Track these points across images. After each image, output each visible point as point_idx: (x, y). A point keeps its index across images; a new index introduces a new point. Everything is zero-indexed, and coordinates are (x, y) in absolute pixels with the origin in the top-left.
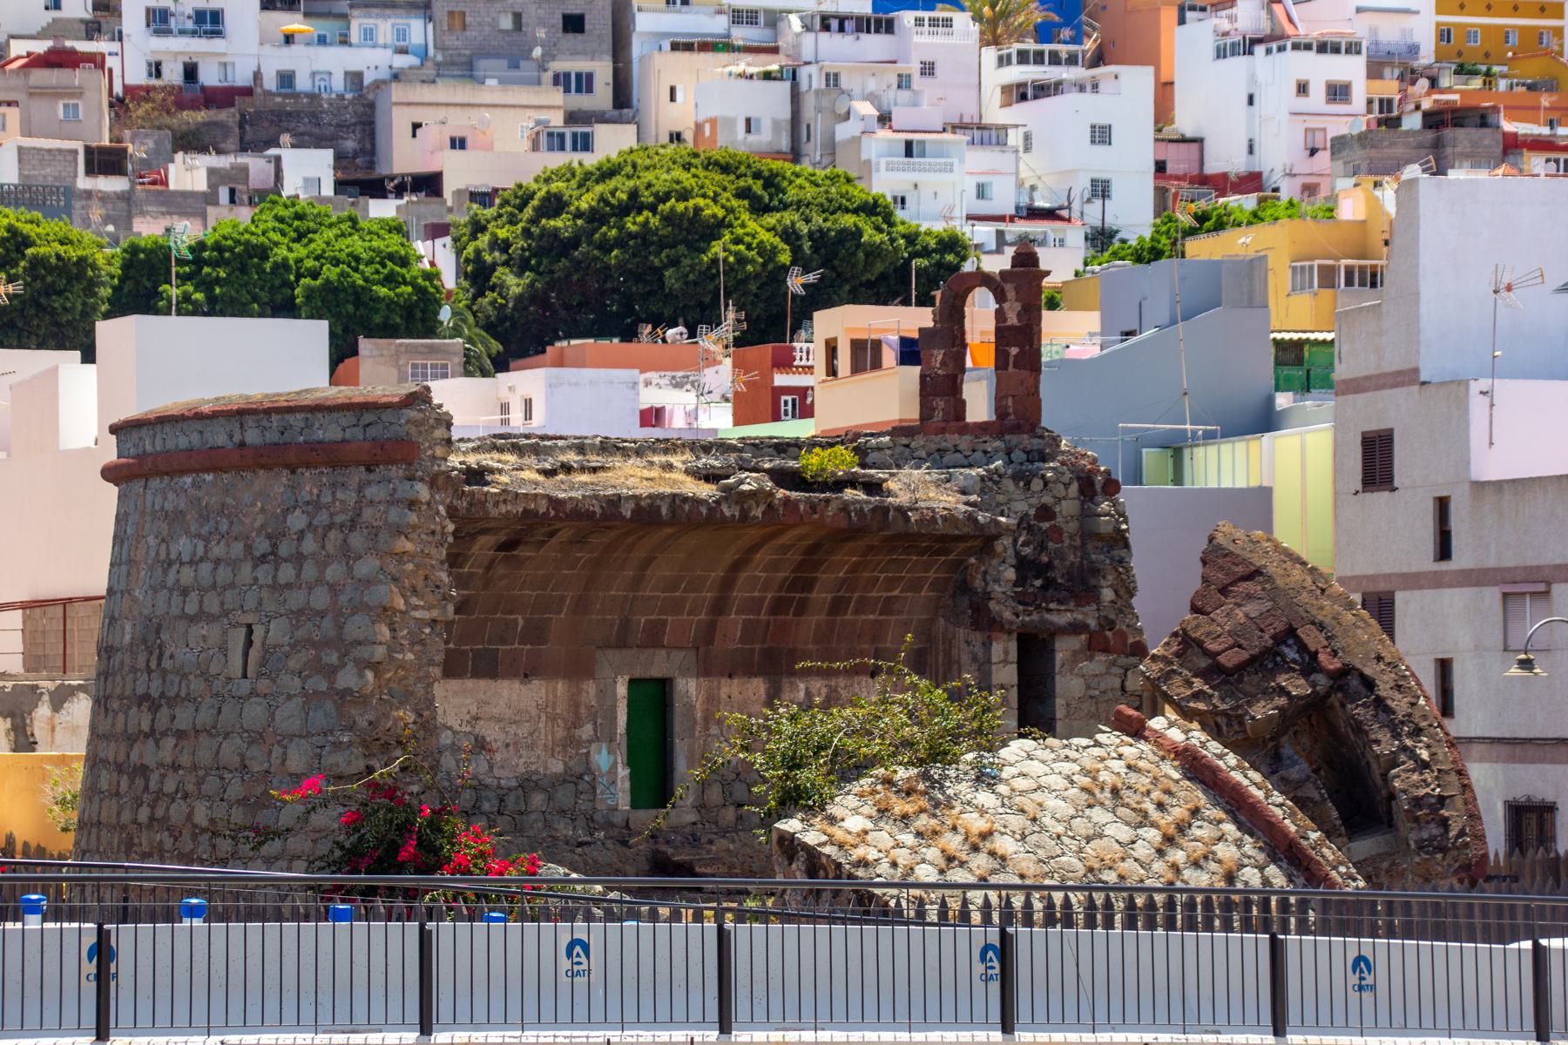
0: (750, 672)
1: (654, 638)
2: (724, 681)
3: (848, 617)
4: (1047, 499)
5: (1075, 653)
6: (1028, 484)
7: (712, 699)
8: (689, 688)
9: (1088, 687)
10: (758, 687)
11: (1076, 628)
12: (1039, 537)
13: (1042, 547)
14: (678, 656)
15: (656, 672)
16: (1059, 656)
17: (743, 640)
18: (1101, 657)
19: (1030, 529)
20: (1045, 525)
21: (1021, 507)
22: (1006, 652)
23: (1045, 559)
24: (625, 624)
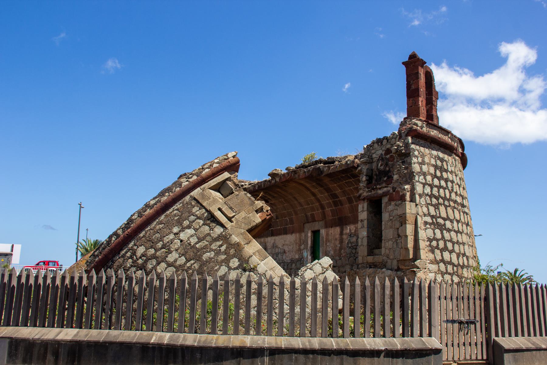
0: (336, 226)
1: (314, 220)
2: (330, 229)
3: (355, 203)
4: (389, 146)
5: (386, 203)
6: (382, 143)
7: (327, 235)
8: (323, 232)
9: (390, 216)
10: (338, 229)
11: (385, 194)
12: (385, 161)
13: (387, 165)
14: (321, 223)
15: (316, 229)
16: (383, 205)
17: (332, 216)
18: (393, 203)
19: (382, 159)
20: (388, 156)
21: (380, 152)
22: (363, 208)
23: (388, 169)
24: (306, 216)
